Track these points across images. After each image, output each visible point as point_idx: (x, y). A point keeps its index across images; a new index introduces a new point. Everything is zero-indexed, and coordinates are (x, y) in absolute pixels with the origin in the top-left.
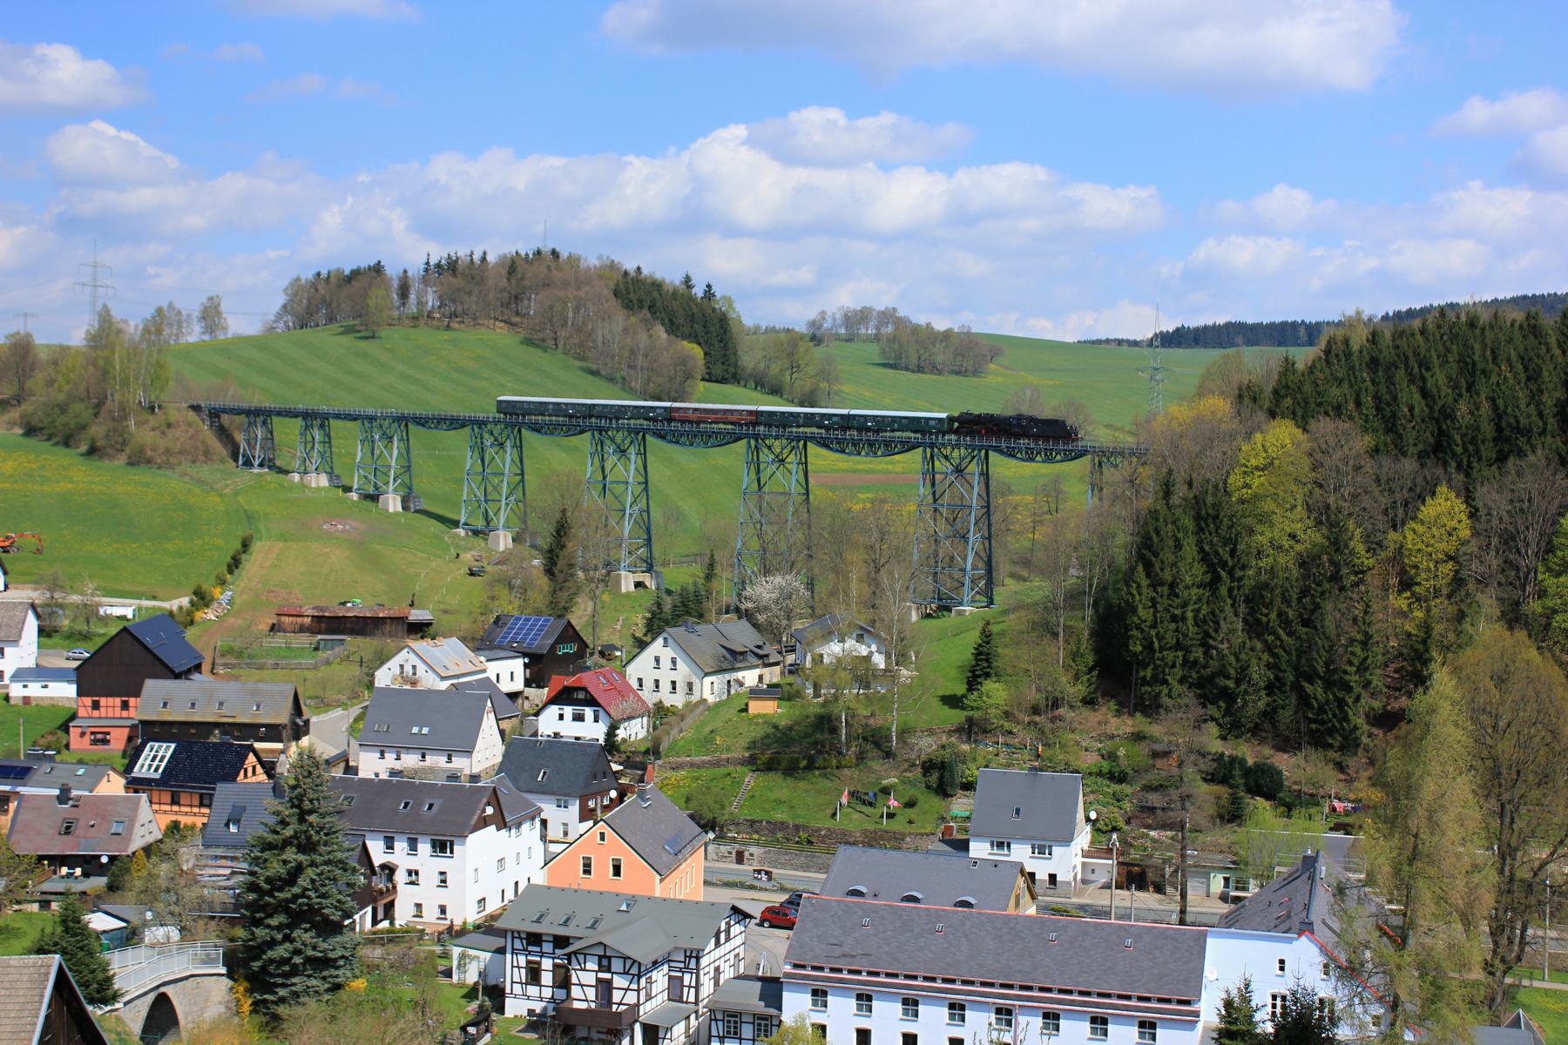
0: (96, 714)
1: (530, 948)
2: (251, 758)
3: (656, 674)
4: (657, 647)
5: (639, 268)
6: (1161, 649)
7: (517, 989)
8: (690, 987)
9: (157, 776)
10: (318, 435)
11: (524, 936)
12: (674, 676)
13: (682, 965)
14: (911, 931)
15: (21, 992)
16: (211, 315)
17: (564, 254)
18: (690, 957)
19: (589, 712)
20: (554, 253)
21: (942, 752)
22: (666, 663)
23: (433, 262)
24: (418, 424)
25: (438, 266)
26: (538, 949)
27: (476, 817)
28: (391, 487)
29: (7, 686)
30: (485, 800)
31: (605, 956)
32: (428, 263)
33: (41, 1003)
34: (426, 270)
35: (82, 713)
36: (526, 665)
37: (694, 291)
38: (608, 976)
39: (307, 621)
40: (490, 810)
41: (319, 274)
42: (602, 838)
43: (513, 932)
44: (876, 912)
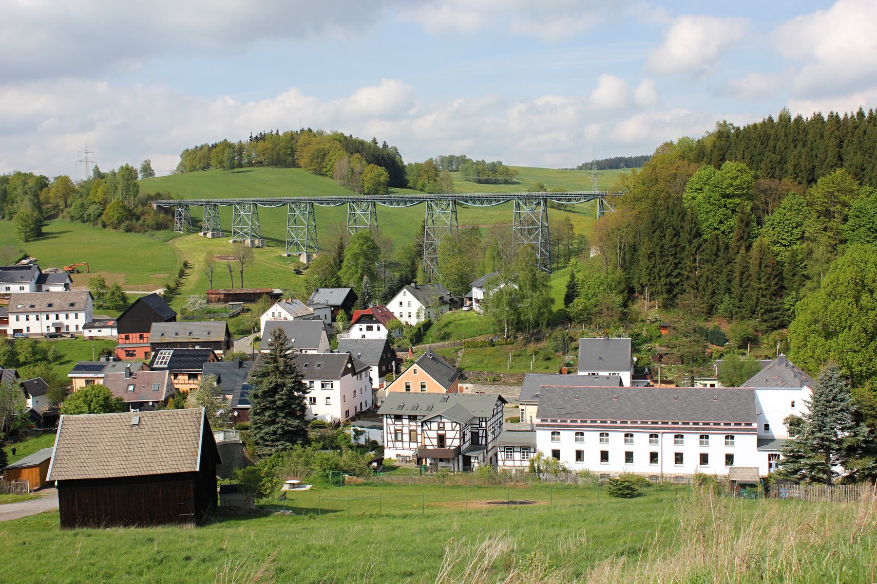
0: (127, 341)
1: (396, 423)
2: (212, 356)
3: (401, 309)
4: (400, 297)
5: (351, 136)
7: (390, 444)
8: (482, 437)
9: (166, 366)
11: (393, 417)
12: (409, 310)
13: (478, 426)
14: (600, 400)
15: (187, 428)
16: (147, 170)
17: (315, 131)
18: (482, 421)
19: (375, 326)
20: (310, 130)
22: (405, 304)
23: (254, 136)
25: (256, 138)
26: (400, 423)
27: (343, 369)
29: (81, 333)
30: (346, 361)
31: (441, 422)
32: (251, 137)
33: (199, 433)
34: (251, 140)
35: (121, 341)
37: (378, 145)
38: (443, 432)
39: (222, 296)
40: (349, 366)
41: (197, 147)
42: (415, 372)
43: (387, 415)
44: (580, 391)
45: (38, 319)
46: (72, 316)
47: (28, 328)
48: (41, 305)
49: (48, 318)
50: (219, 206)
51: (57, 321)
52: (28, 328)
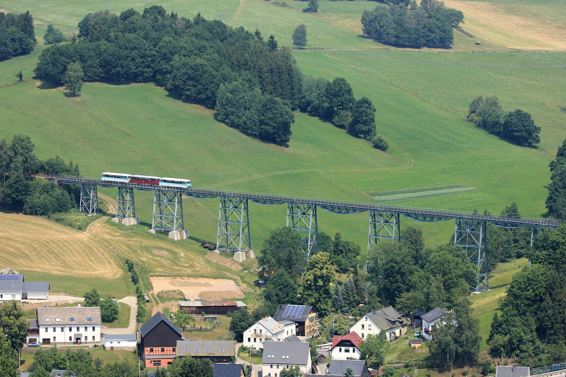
0: (152, 353)
3: (363, 331)
4: (363, 321)
6: (556, 324)
10: (128, 197)
19: (351, 349)
21: (482, 361)
24: (190, 195)
28: (175, 228)
36: (297, 327)
45: (62, 331)
46: (90, 329)
47: (55, 338)
48: (64, 319)
49: (70, 330)
50: (135, 190)
51: (78, 332)
52: (55, 338)
